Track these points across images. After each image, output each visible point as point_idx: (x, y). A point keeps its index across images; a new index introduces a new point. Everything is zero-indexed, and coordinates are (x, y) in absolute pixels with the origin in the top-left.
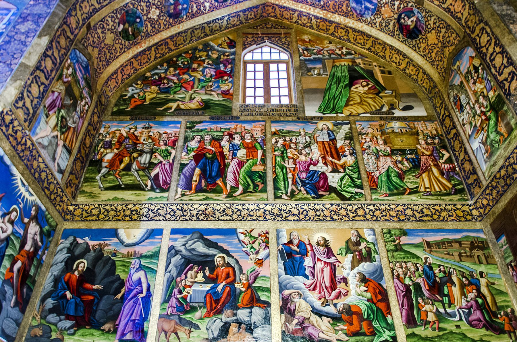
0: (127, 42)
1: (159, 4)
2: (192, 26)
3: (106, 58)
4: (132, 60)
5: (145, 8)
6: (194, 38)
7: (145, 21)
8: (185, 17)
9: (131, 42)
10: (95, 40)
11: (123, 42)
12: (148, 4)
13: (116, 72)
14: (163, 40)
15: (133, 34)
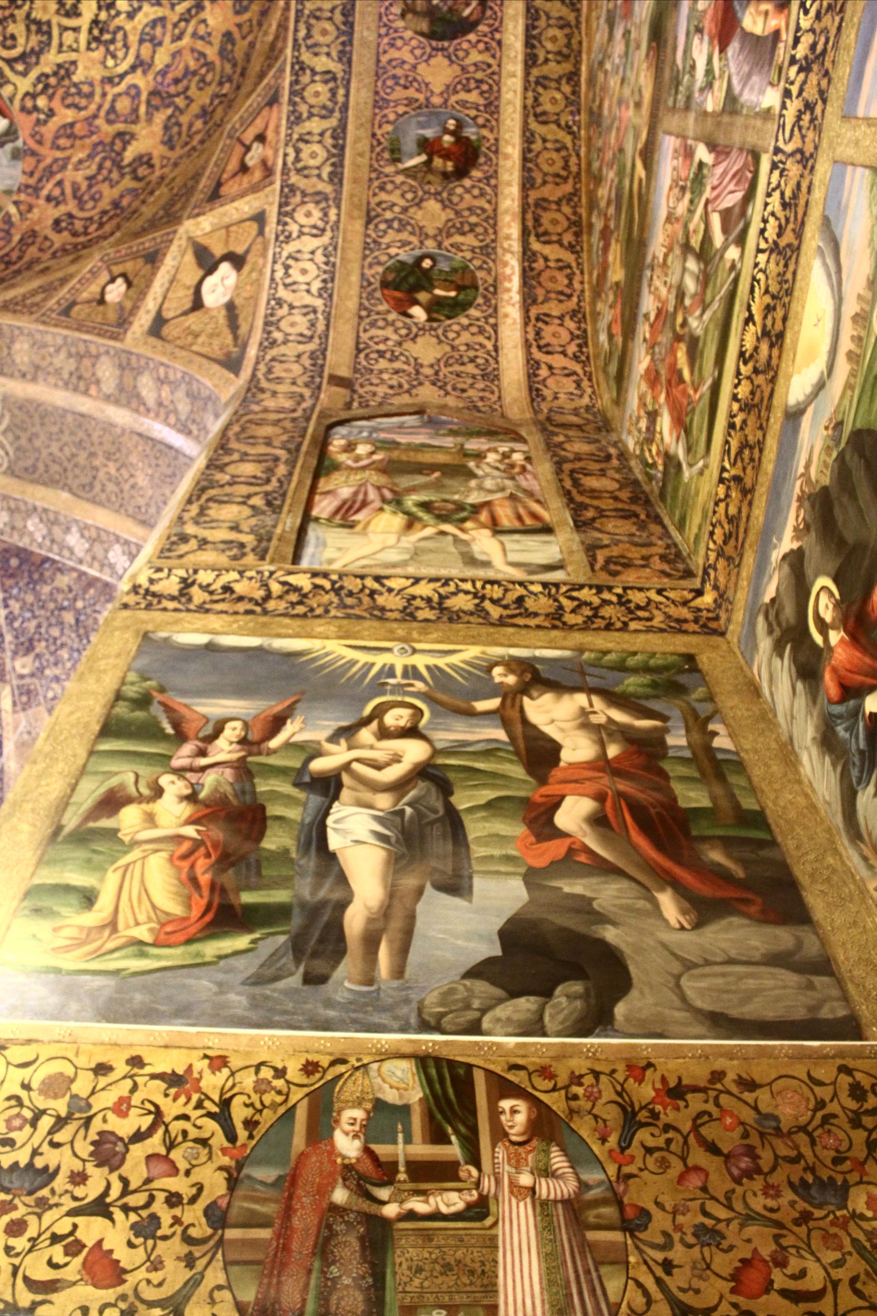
0: (473, 312)
1: (409, 196)
2: (518, 117)
3: (474, 377)
4: (533, 312)
5: (404, 236)
6: (566, 118)
7: (440, 245)
8: (485, 132)
9: (480, 300)
10: (394, 382)
11: (465, 321)
12: (396, 225)
13: (532, 366)
14: (524, 212)
15: (460, 288)
